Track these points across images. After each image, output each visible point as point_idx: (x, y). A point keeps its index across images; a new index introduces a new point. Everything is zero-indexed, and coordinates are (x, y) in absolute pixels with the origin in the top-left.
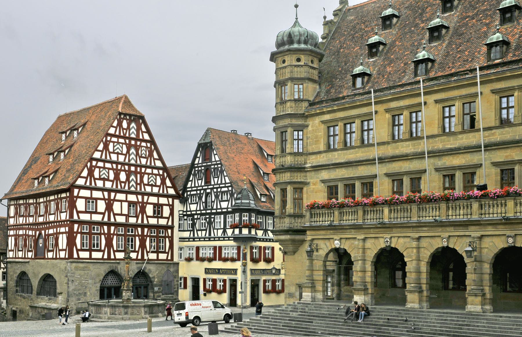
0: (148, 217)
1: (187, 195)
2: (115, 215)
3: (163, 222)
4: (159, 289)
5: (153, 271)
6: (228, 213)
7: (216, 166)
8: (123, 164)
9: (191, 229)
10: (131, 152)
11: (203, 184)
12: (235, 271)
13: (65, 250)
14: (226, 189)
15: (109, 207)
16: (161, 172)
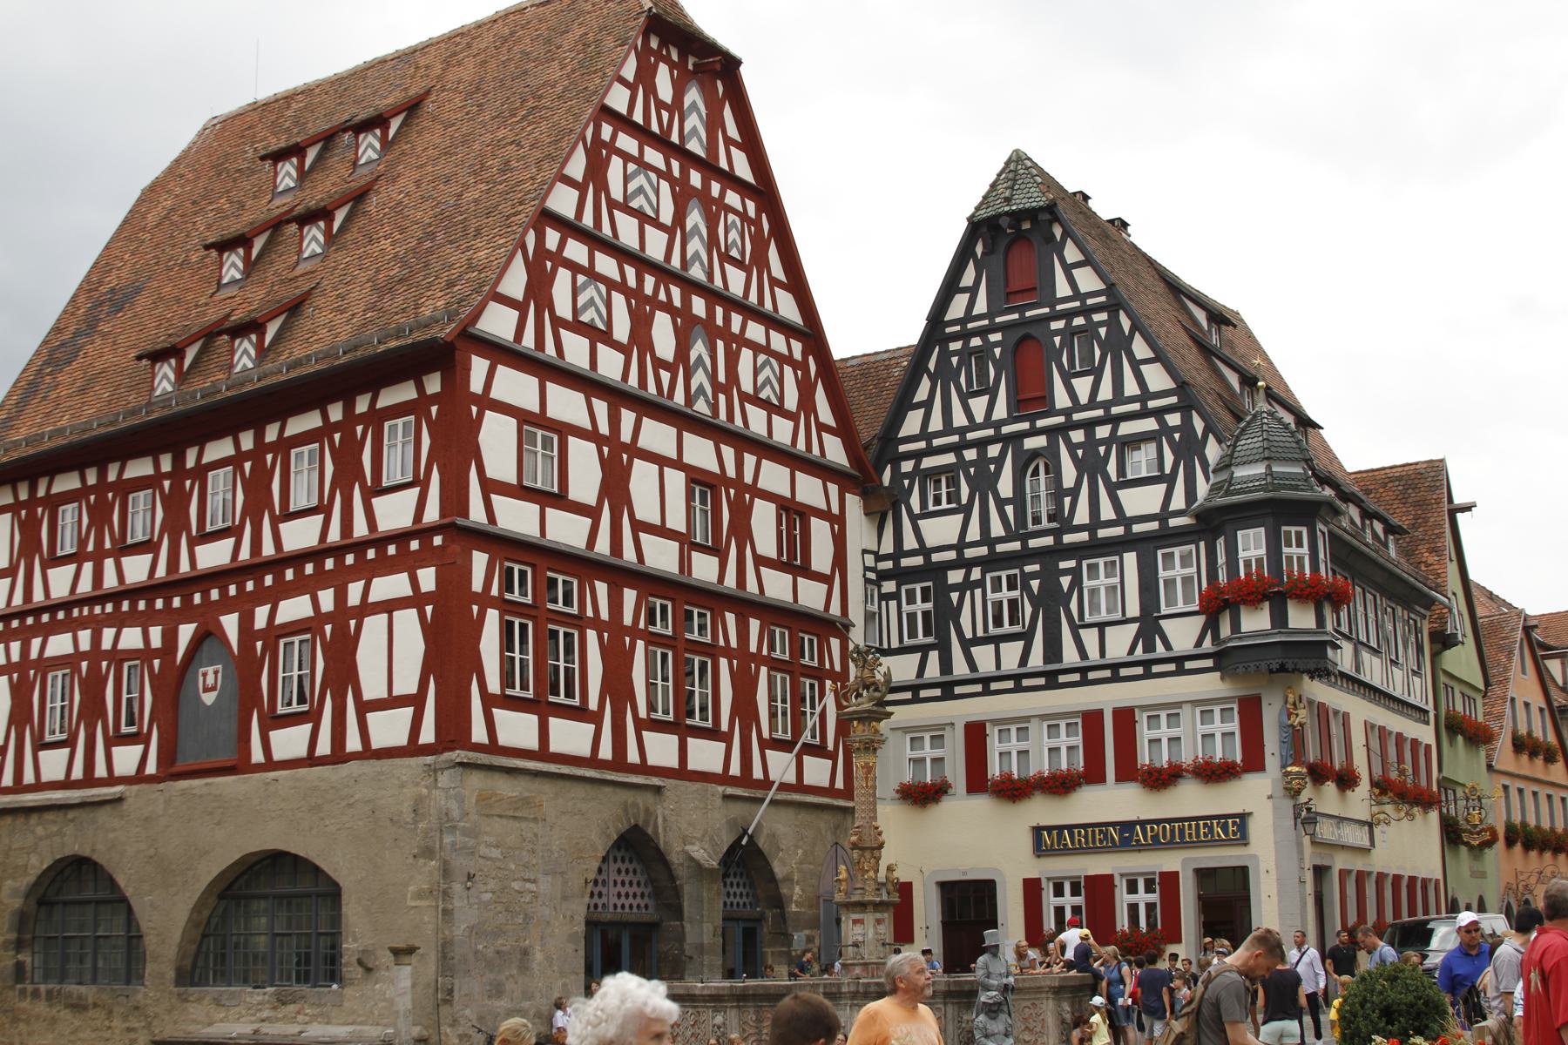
0: (760, 561)
1: (897, 476)
2: (639, 527)
3: (812, 596)
4: (810, 939)
5: (791, 848)
6: (1168, 537)
7: (1079, 321)
8: (663, 273)
9: (921, 639)
10: (689, 225)
11: (1000, 411)
12: (1237, 826)
13: (417, 701)
14: (1150, 424)
15: (615, 486)
16: (797, 347)
